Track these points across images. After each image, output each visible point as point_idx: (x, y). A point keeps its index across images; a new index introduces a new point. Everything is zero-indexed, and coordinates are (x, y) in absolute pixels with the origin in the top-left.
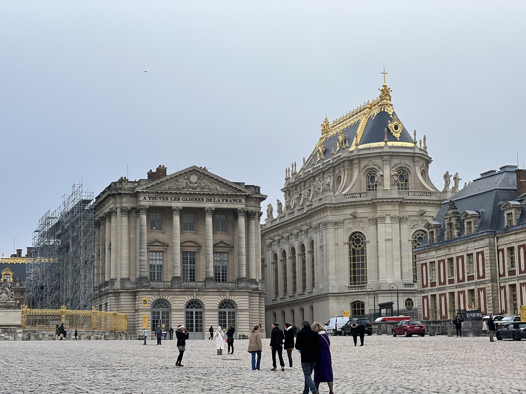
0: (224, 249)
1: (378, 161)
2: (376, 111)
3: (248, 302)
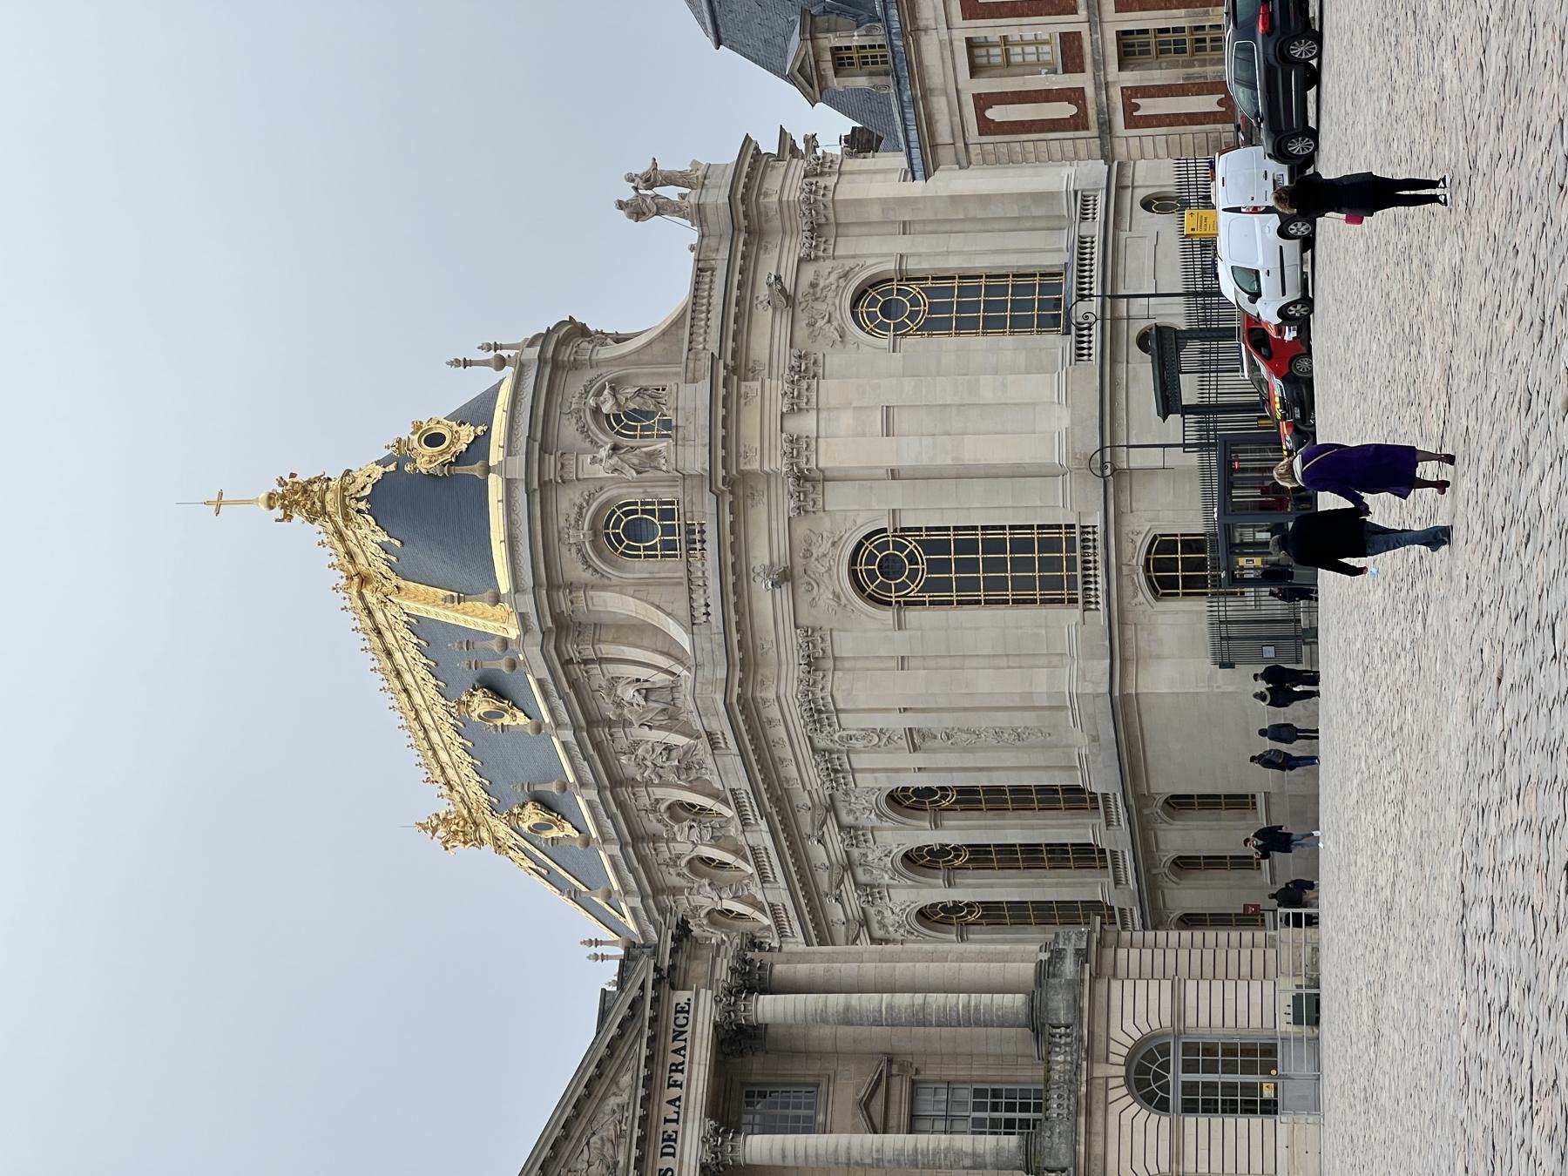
0: (895, 1097)
1: (566, 502)
2: (369, 537)
3: (1141, 984)
